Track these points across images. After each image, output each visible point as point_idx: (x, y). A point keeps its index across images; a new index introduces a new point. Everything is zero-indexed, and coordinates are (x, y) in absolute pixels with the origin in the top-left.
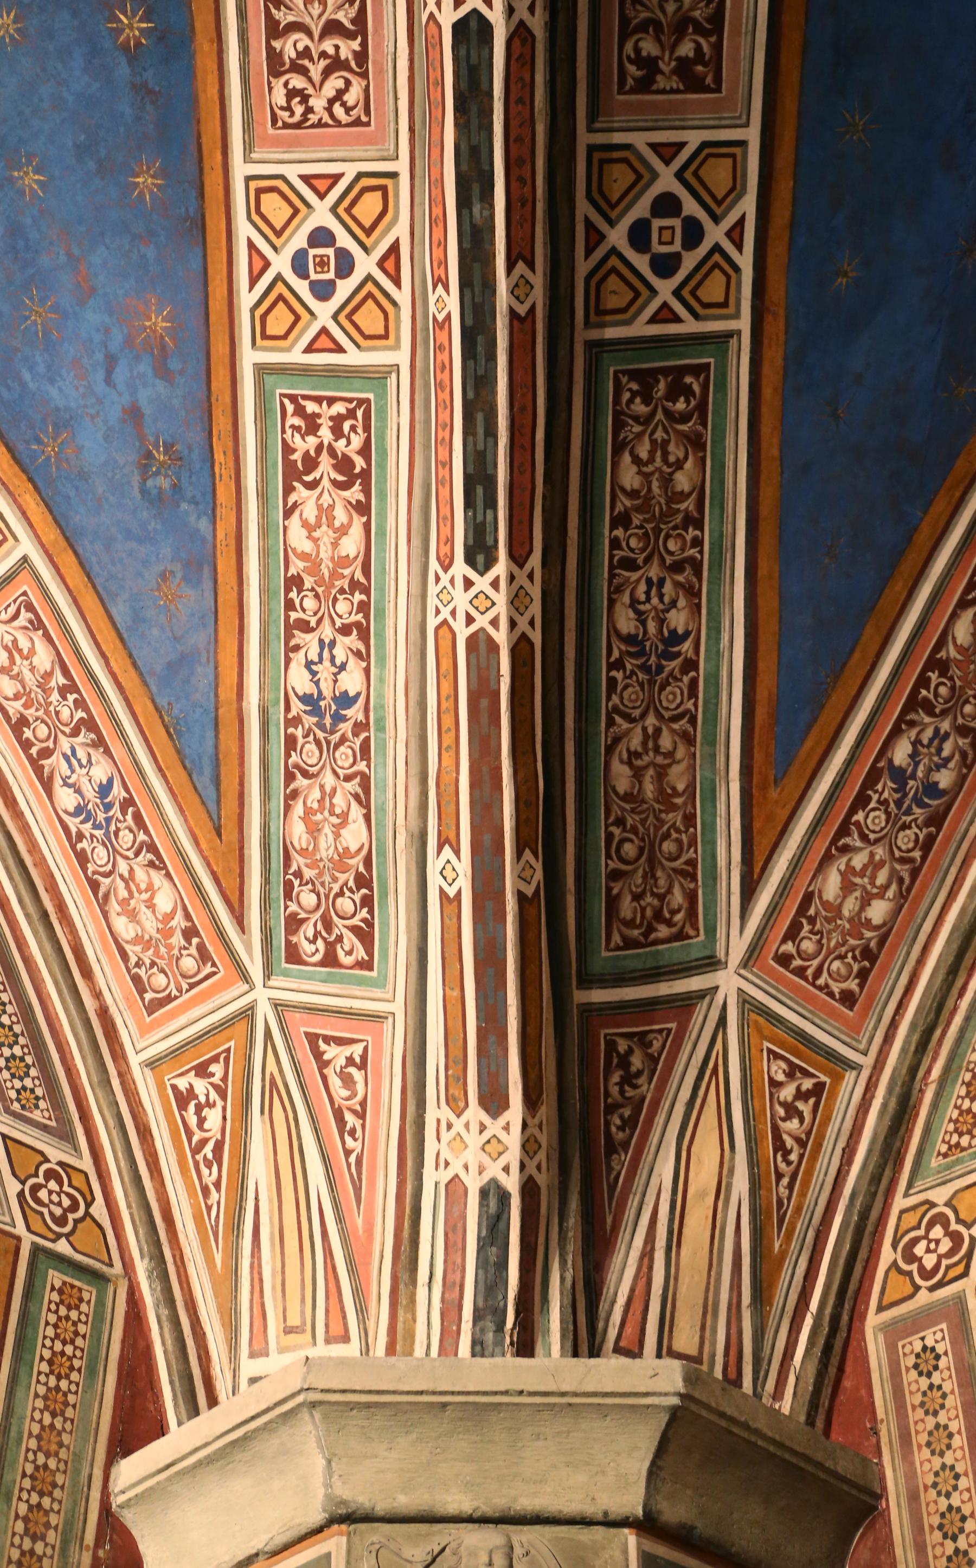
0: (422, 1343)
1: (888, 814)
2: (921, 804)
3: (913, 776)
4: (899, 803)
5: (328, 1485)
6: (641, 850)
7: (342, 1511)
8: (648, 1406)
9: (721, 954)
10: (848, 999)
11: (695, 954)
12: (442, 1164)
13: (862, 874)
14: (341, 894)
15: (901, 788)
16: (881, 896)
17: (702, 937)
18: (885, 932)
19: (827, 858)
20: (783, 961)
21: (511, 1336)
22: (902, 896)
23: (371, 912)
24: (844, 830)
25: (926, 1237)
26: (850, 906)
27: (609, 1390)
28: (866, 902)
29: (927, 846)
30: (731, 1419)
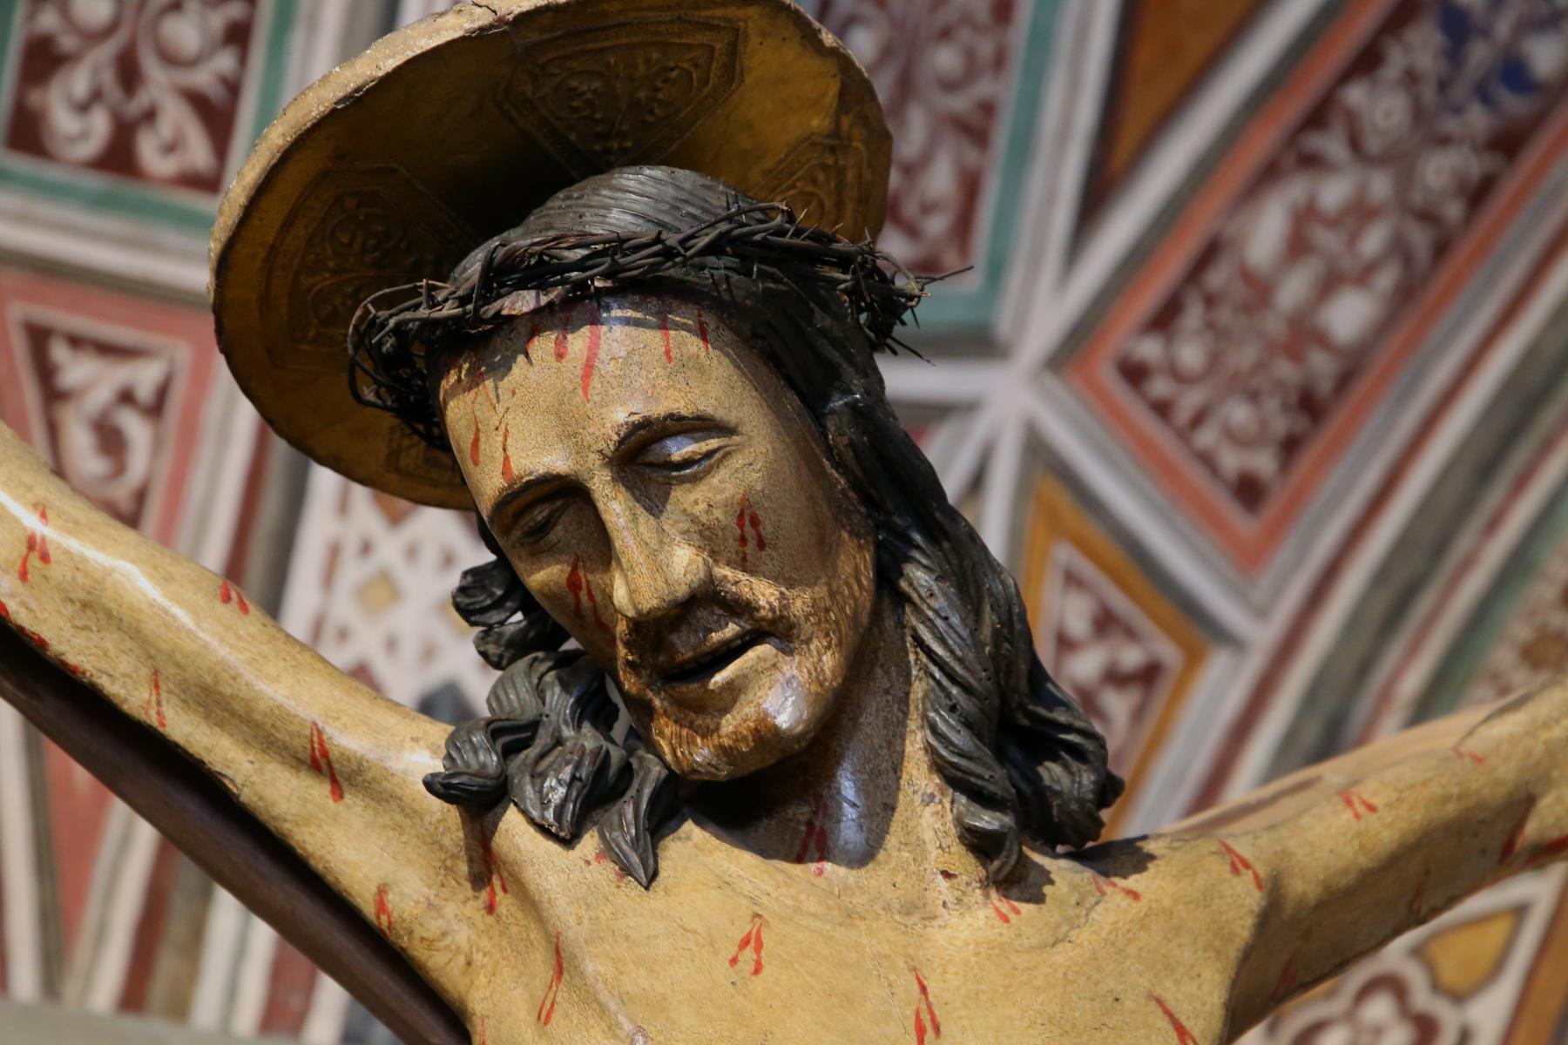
3: (1486, 33)
4: (1443, 86)
9: (1004, 325)
10: (1249, 491)
12: (329, 632)
13: (1333, 223)
15: (1455, 53)
16: (1363, 276)
17: (972, 283)
19: (1269, 174)
20: (1135, 374)
22: (1406, 295)
23: (243, 59)
24: (1317, 118)
26: (1293, 290)
28: (1329, 285)
29: (1478, 194)
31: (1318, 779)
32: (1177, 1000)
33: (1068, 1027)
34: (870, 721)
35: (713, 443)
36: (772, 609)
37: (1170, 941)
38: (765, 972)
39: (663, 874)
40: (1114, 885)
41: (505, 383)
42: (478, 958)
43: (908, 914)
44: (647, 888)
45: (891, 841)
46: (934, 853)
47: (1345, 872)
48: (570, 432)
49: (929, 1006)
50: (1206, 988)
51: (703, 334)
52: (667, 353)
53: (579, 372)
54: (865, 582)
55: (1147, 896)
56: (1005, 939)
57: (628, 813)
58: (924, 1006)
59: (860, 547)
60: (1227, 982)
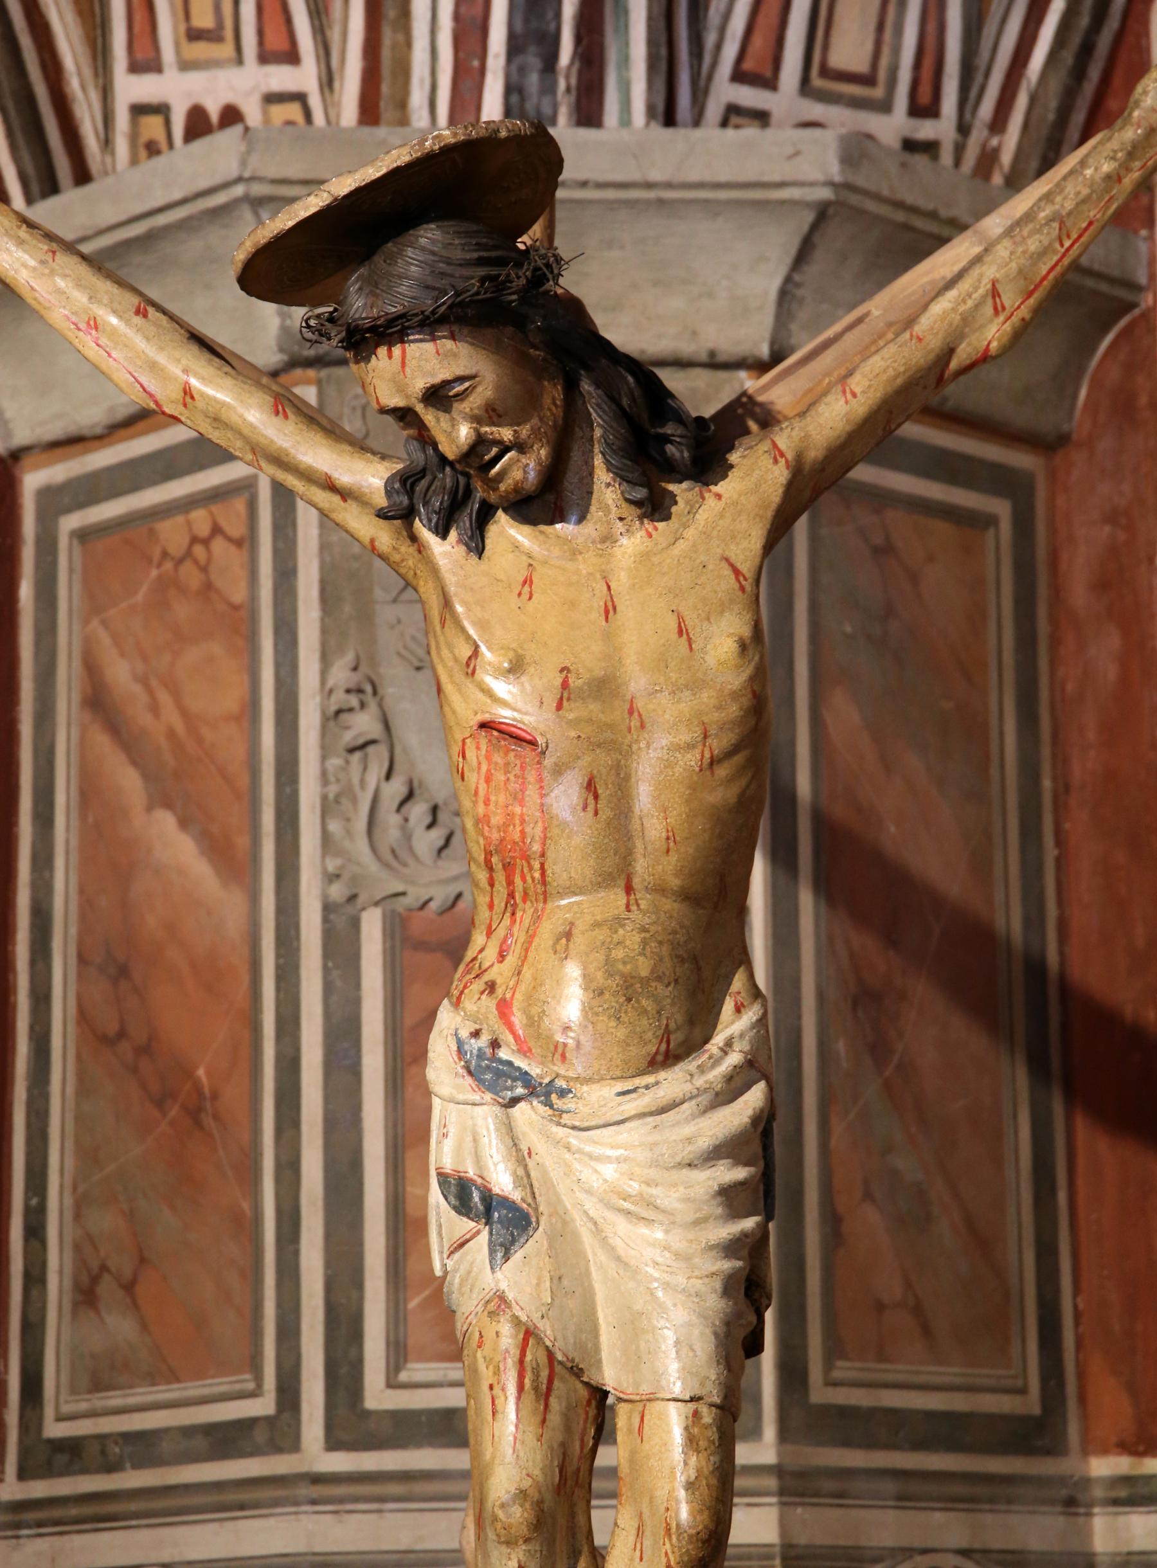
0: (422, 81)
8: (782, 202)
21: (567, 78)
27: (723, 178)
30: (914, 210)
31: (867, 314)
32: (736, 555)
33: (677, 592)
34: (576, 456)
35: (467, 384)
36: (510, 441)
37: (735, 520)
38: (534, 598)
39: (488, 547)
40: (710, 491)
41: (369, 365)
42: (418, 572)
43: (604, 542)
44: (480, 559)
45: (593, 509)
46: (614, 509)
47: (839, 437)
48: (401, 389)
49: (612, 598)
50: (753, 542)
51: (453, 337)
52: (437, 352)
53: (400, 364)
54: (558, 403)
55: (725, 496)
56: (649, 548)
58: (609, 598)
59: (555, 385)
60: (765, 533)
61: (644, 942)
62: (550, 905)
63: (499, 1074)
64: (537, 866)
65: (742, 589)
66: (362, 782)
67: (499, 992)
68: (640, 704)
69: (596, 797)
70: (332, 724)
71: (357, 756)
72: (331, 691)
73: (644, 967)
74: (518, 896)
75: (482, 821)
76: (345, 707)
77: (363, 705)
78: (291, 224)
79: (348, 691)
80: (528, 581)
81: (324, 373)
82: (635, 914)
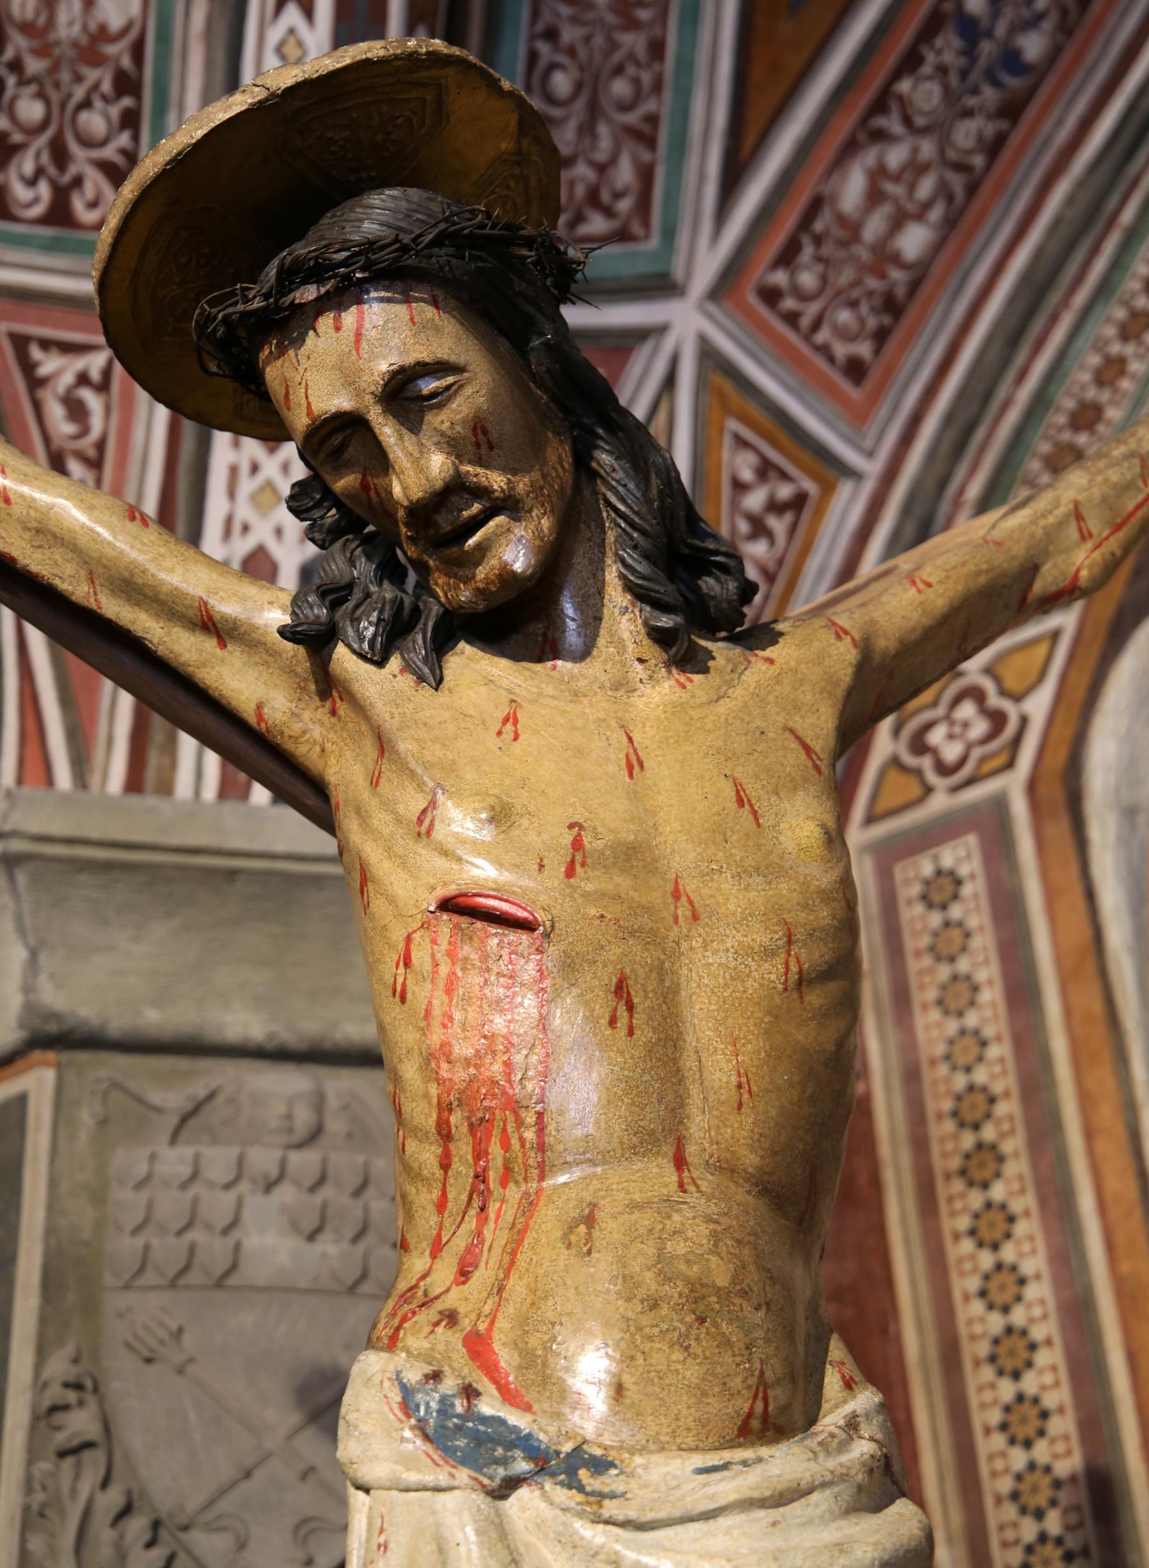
1: (946, 88)
2: (996, 83)
3: (989, 34)
4: (964, 74)
5: (28, 988)
6: (578, 87)
7: (52, 1028)
9: (678, 273)
10: (855, 370)
11: (643, 267)
12: (237, 528)
13: (897, 178)
14: (86, 104)
15: (970, 51)
16: (920, 216)
17: (654, 243)
18: (920, 273)
19: (851, 148)
20: (771, 296)
22: (950, 223)
23: (136, 138)
24: (880, 106)
25: (948, 718)
26: (874, 227)
28: (898, 222)
29: (994, 148)
31: (895, 567)
32: (803, 729)
33: (730, 755)
34: (580, 561)
35: (450, 379)
36: (503, 491)
37: (796, 689)
38: (521, 738)
39: (447, 679)
40: (757, 656)
41: (303, 351)
42: (328, 746)
43: (617, 690)
44: (436, 690)
45: (601, 641)
46: (631, 647)
47: (913, 630)
48: (349, 379)
49: (635, 750)
50: (823, 718)
51: (435, 304)
52: (412, 319)
53: (352, 338)
54: (566, 466)
55: (779, 661)
56: (684, 700)
57: (419, 640)
58: (631, 751)
59: (561, 442)
60: (837, 713)
61: (715, 1236)
62: (548, 1183)
63: (479, 1440)
64: (530, 1119)
65: (817, 768)
66: (74, 1492)
67: (466, 1323)
68: (690, 886)
69: (630, 1008)
70: (43, 1424)
71: (69, 1462)
72: (45, 1385)
73: (721, 1274)
74: (493, 1177)
75: (433, 1058)
76: (61, 1402)
77: (81, 1404)
78: (200, 134)
79: (67, 1385)
80: (511, 718)
81: (66, 1056)
82: (693, 1198)
